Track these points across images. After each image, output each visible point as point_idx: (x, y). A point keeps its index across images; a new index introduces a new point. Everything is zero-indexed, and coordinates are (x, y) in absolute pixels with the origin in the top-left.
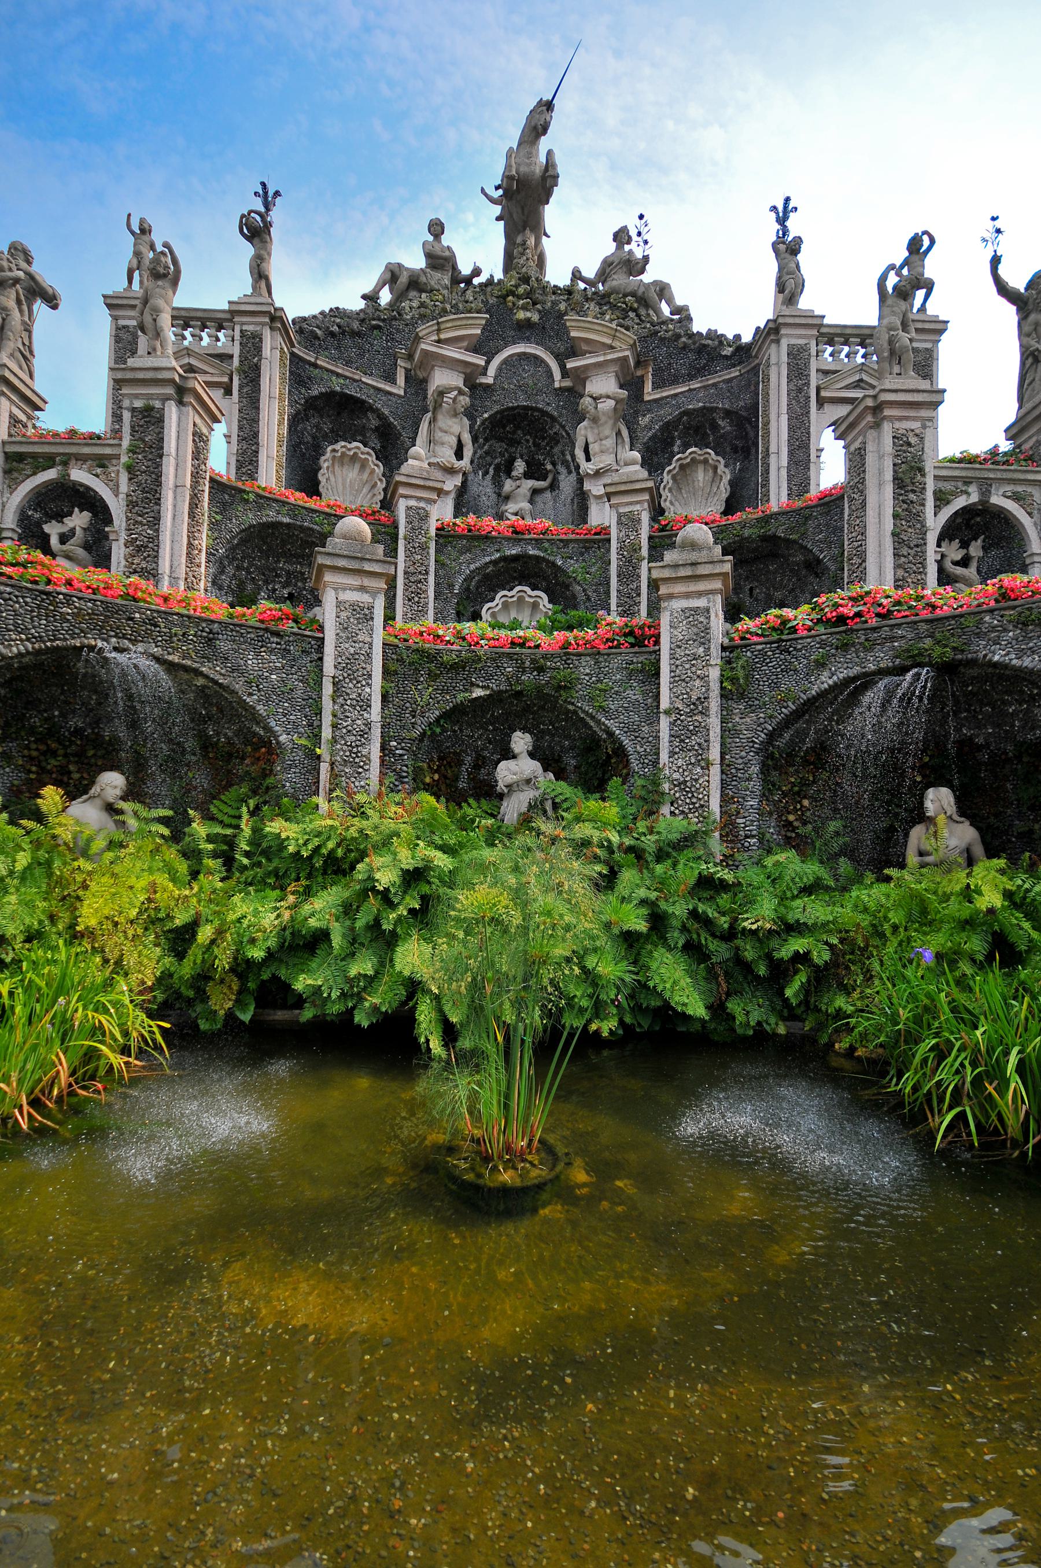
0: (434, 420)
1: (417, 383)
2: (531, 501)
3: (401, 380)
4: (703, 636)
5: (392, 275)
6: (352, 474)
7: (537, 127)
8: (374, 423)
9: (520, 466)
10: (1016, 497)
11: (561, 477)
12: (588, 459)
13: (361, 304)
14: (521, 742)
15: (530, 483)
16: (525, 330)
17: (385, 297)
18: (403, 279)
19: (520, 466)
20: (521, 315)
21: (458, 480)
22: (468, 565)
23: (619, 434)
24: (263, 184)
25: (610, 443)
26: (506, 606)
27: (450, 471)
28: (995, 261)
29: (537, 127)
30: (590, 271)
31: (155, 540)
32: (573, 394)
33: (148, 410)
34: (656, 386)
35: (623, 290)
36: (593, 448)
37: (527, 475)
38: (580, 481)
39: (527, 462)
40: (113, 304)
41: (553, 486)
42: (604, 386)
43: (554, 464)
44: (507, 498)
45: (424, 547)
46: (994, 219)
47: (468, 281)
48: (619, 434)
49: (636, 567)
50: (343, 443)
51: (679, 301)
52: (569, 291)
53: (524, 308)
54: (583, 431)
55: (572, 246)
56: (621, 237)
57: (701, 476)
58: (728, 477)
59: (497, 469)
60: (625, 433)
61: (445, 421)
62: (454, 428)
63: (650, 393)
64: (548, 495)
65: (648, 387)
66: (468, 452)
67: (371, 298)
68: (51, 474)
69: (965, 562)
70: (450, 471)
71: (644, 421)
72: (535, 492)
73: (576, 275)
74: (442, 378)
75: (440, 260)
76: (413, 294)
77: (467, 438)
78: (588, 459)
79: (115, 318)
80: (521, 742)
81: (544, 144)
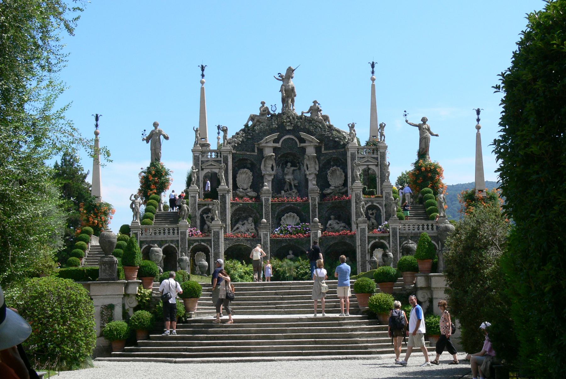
0: (265, 161)
1: (261, 151)
2: (293, 173)
3: (256, 151)
4: (316, 236)
5: (252, 118)
6: (244, 176)
7: (290, 71)
8: (249, 162)
9: (289, 164)
10: (378, 203)
11: (302, 167)
12: (308, 169)
13: (243, 127)
14: (291, 252)
15: (293, 168)
16: (289, 132)
17: (250, 123)
18: (256, 120)
19: (289, 164)
20: (288, 129)
21: (272, 177)
22: (278, 210)
23: (315, 162)
24: (202, 66)
25: (313, 165)
26: (287, 217)
27: (270, 175)
28: (407, 121)
29: (290, 71)
30: (307, 111)
31: (226, 219)
32: (303, 150)
33: (223, 195)
34: (325, 150)
35: (314, 123)
36: (309, 166)
37: (291, 166)
38: (306, 175)
39: (291, 162)
40: (193, 151)
41: (300, 169)
42: (311, 151)
43: (299, 163)
44: (286, 174)
45: (268, 207)
46: (405, 111)
47: (272, 115)
48: (315, 162)
49: (315, 210)
50: (242, 170)
51: (331, 124)
52: (301, 118)
53: (289, 126)
54: (306, 162)
55: (300, 107)
56: (315, 102)
57: (338, 172)
58: (344, 175)
59: (282, 164)
60: (317, 162)
61: (268, 162)
62: (271, 163)
63: (323, 151)
64: (298, 171)
65: (323, 149)
66: (275, 168)
67: (246, 126)
68: (206, 207)
69: (372, 214)
70: (270, 175)
71: (322, 158)
72: (294, 170)
73: (302, 113)
74: (269, 152)
75: (265, 111)
76: (258, 123)
77: (274, 164)
78: (308, 169)
79: (194, 154)
80: (291, 252)
81: (292, 82)
